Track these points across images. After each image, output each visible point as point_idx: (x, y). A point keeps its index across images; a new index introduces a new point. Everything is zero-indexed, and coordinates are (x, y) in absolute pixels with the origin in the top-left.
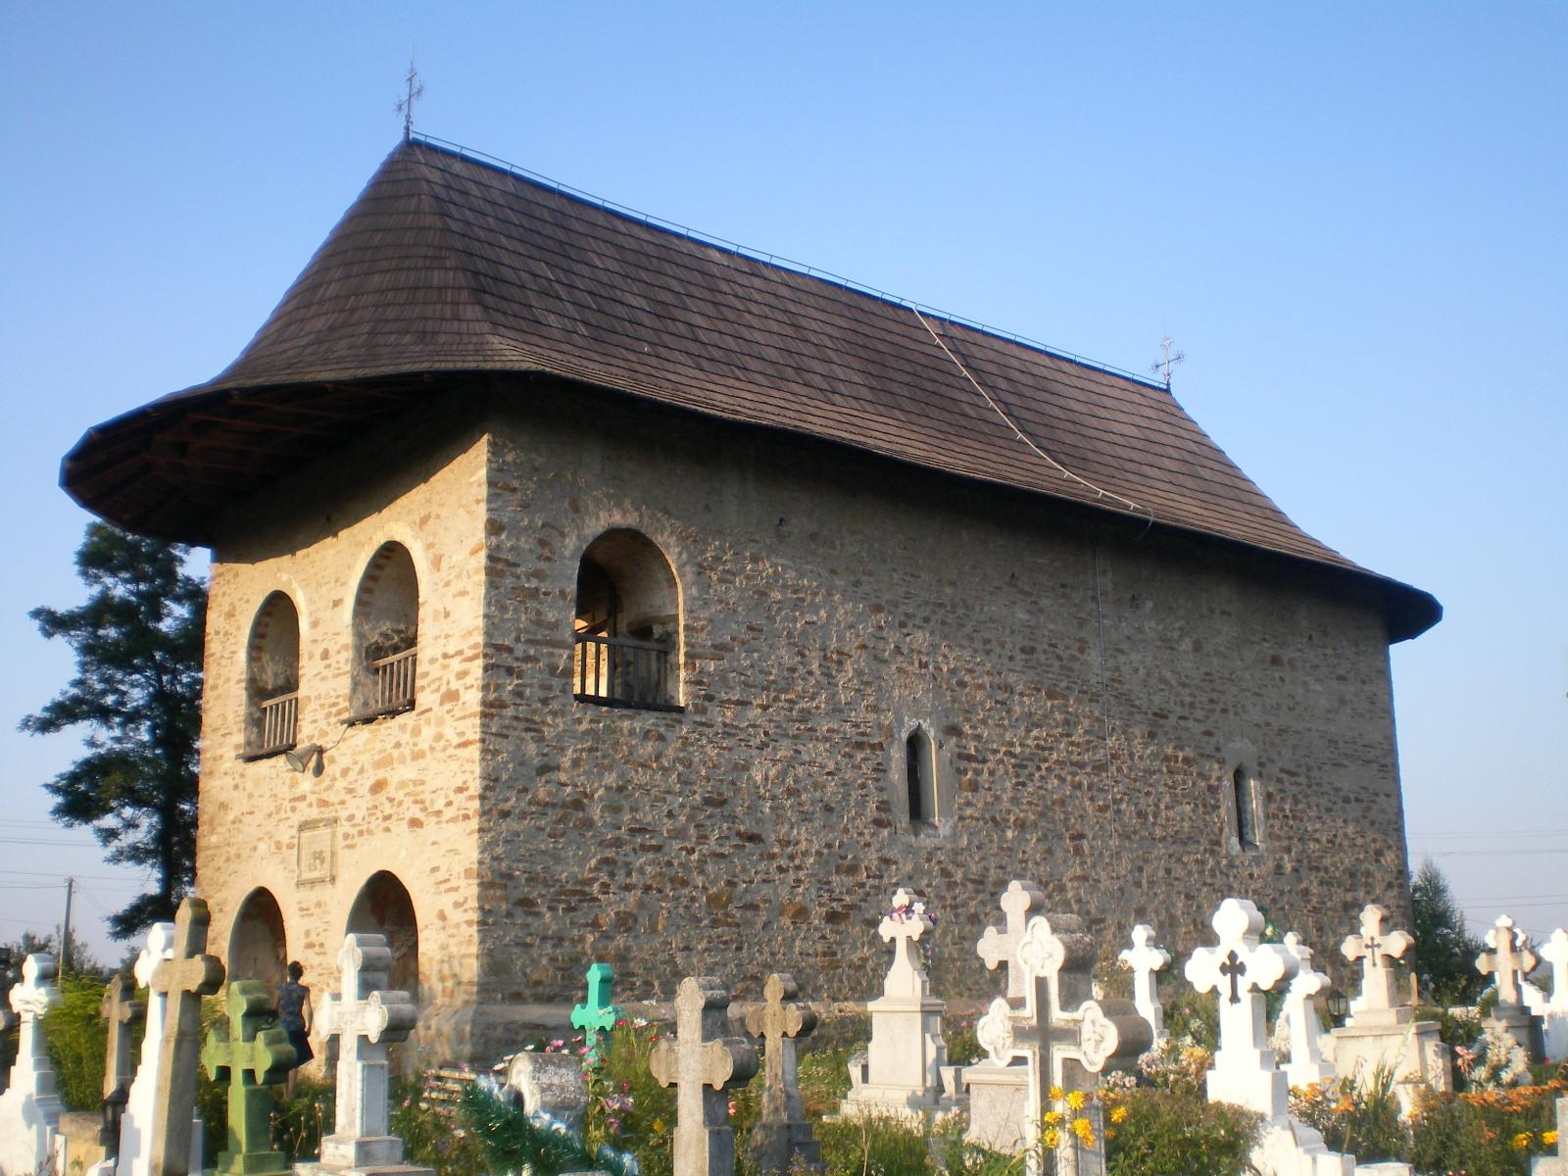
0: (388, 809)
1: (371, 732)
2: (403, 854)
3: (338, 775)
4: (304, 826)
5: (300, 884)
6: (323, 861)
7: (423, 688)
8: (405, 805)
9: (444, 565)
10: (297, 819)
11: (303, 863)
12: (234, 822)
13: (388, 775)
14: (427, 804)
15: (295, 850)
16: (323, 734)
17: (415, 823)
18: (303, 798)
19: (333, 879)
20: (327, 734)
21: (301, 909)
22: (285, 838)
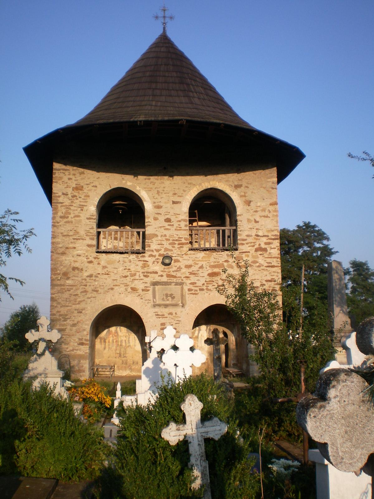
1: (205, 254)
3: (183, 267)
4: (155, 284)
5: (154, 306)
7: (243, 244)
9: (252, 204)
12: (87, 277)
15: (150, 292)
16: (166, 249)
18: (156, 273)
20: (172, 250)
21: (157, 315)
22: (140, 286)
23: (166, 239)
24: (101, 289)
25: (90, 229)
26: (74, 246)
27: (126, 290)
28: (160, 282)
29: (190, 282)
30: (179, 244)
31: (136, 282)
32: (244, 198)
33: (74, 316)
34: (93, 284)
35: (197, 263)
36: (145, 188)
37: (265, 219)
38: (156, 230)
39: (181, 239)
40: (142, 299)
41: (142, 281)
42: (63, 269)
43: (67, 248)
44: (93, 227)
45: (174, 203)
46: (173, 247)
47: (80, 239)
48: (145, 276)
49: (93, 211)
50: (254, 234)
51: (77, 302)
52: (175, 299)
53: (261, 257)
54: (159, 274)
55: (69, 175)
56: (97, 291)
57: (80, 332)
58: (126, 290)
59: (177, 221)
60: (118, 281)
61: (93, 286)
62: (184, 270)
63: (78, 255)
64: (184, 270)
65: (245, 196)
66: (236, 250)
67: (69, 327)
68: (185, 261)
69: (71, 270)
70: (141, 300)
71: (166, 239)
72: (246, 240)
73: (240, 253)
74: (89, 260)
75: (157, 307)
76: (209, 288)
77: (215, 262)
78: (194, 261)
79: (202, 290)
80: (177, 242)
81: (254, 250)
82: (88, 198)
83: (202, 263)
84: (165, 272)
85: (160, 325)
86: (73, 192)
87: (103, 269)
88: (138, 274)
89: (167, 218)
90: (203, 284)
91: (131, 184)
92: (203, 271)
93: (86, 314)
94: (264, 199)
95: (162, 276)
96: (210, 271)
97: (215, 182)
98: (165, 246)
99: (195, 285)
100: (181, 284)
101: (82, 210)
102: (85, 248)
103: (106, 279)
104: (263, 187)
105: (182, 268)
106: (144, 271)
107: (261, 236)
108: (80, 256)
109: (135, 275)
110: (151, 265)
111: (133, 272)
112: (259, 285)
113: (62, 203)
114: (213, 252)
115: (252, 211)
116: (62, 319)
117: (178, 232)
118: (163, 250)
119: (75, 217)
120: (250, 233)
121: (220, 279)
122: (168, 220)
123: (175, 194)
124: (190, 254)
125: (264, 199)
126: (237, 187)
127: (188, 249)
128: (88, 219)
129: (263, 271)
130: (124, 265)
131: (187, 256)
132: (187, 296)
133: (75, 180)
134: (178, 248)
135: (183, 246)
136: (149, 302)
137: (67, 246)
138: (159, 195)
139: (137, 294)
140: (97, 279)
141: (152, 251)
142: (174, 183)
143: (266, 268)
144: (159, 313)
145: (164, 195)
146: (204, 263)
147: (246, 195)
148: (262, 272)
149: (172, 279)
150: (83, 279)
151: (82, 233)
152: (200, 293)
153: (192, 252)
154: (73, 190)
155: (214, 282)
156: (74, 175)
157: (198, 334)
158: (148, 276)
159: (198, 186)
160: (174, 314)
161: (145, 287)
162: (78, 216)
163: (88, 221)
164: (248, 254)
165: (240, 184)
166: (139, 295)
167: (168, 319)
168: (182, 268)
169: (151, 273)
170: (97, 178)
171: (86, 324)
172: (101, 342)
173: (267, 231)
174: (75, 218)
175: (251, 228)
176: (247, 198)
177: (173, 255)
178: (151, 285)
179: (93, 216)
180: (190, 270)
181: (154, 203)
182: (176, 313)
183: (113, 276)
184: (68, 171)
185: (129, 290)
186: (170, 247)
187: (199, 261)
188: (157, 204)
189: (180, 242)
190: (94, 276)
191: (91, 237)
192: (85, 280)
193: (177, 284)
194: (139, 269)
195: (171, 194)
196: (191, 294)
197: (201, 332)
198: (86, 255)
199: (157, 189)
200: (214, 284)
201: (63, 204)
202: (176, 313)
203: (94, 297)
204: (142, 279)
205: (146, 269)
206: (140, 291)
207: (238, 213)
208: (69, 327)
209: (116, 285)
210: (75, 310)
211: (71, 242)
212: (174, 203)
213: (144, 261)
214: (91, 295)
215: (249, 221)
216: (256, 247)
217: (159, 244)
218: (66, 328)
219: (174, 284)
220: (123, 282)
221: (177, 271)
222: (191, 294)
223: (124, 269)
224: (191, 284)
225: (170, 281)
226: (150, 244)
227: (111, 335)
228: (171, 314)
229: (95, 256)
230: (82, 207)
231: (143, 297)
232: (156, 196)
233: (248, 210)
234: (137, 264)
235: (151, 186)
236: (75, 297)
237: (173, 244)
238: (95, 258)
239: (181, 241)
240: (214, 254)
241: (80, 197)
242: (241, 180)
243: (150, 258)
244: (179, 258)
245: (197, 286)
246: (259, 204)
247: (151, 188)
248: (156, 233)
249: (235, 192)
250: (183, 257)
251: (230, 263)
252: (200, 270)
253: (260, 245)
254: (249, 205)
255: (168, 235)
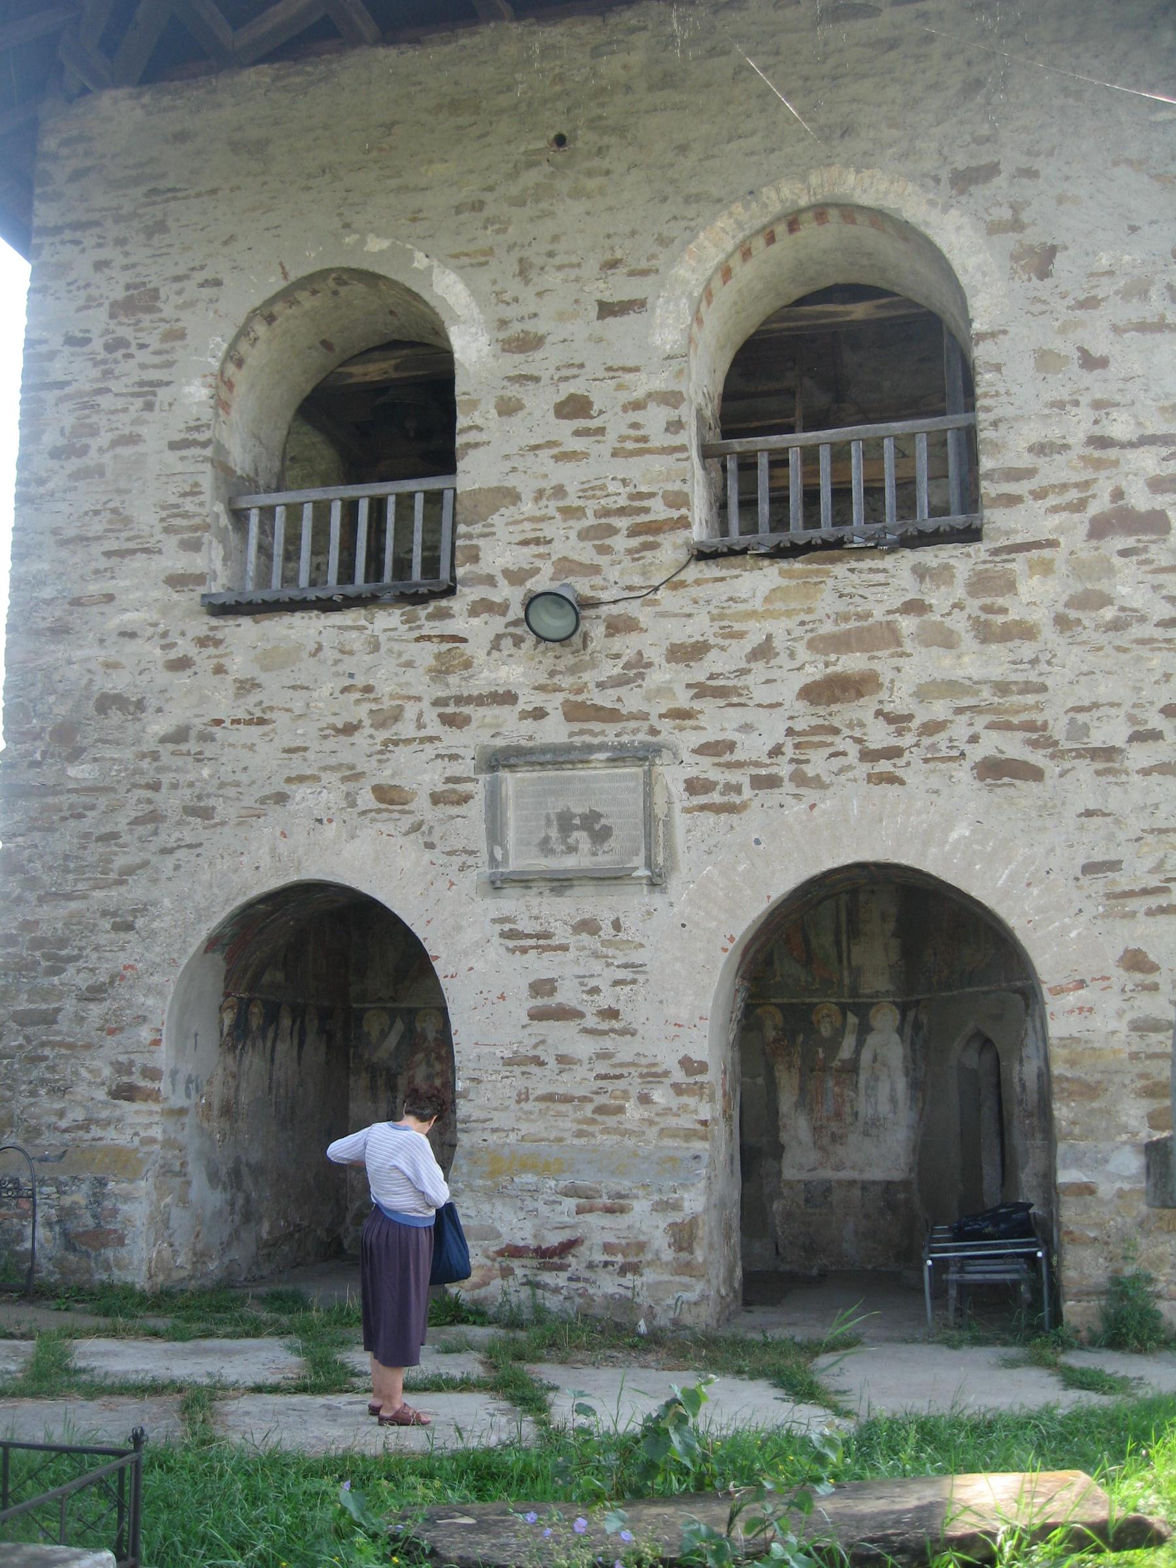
0: (879, 736)
1: (782, 573)
2: (961, 831)
3: (656, 654)
4: (498, 761)
5: (497, 884)
6: (601, 836)
7: (1012, 500)
8: (960, 729)
9: (1060, 262)
10: (469, 742)
11: (511, 836)
12: (164, 740)
13: (876, 666)
14: (1058, 730)
15: (476, 809)
16: (566, 566)
17: (995, 770)
18: (509, 698)
19: (656, 882)
20: (596, 569)
22: (421, 774)
23: (559, 509)
24: (226, 798)
25: (185, 495)
26: (108, 586)
27: (351, 800)
28: (531, 751)
29: (697, 739)
30: (633, 532)
31: (401, 754)
32: (1010, 241)
33: (97, 948)
34: (190, 777)
35: (737, 627)
36: (456, 256)
37: (1149, 339)
38: (509, 465)
39: (645, 503)
40: (430, 846)
41: (430, 750)
42: (56, 710)
43: (77, 602)
44: (196, 484)
45: (607, 310)
46: (604, 550)
47: (133, 552)
48: (449, 721)
49: (199, 404)
50: (1077, 438)
51: (113, 876)
52: (612, 843)
53: (1127, 568)
54: (521, 705)
55: (99, 245)
56: (205, 814)
57: (120, 1029)
58: (351, 800)
59: (625, 409)
60: (310, 755)
61: (191, 785)
62: (661, 675)
63: (123, 634)
64: (661, 675)
65: (1017, 225)
66: (972, 534)
67: (70, 1005)
68: (670, 625)
69: (90, 708)
70: (428, 855)
71: (559, 509)
72: (1030, 473)
73: (996, 552)
74: (173, 655)
75: (509, 891)
76: (810, 771)
77: (846, 618)
78: (721, 617)
79: (772, 782)
80: (622, 523)
81: (1084, 529)
82: (178, 344)
83: (769, 626)
84: (558, 689)
85: (525, 991)
86: (112, 325)
87: (238, 696)
88: (411, 710)
89: (572, 398)
90: (776, 751)
91: (385, 244)
92: (775, 674)
93: (153, 934)
94: (1133, 229)
95: (539, 714)
96: (814, 672)
97: (835, 170)
98: (559, 549)
99: (727, 758)
100: (646, 755)
101: (149, 406)
102: (156, 594)
103: (251, 748)
104: (1129, 162)
105: (649, 665)
106: (441, 693)
107: (1123, 446)
108: (133, 635)
109: (397, 716)
110: (480, 657)
111: (387, 704)
112: (1120, 742)
113: (62, 385)
114: (833, 561)
115: (1060, 306)
116: (45, 964)
117: (633, 469)
118: (547, 569)
119: (115, 443)
120: (1054, 433)
121: (879, 713)
122: (575, 407)
123: (613, 264)
124: (698, 582)
125: (1133, 229)
126: (965, 180)
127: (683, 556)
128: (173, 446)
129: (1144, 652)
130: (340, 668)
131: (681, 592)
132: (680, 821)
133: (126, 268)
134: (629, 551)
135: (660, 538)
136: (470, 860)
137: (76, 594)
138: (527, 283)
139: (407, 822)
140: (209, 750)
141: (490, 581)
142: (610, 209)
143: (1159, 633)
144: (519, 927)
145: (553, 279)
146: (778, 628)
147: (1025, 217)
148: (1139, 659)
149: (596, 726)
150: (143, 756)
151: (146, 518)
152: (756, 804)
153: (710, 570)
154: (112, 316)
155: (836, 731)
156: (121, 242)
157: (858, 1051)
158: (467, 720)
159: (738, 208)
160: (607, 931)
161: (449, 780)
162: (133, 439)
163: (171, 457)
164: (1047, 553)
165: (984, 160)
166: (416, 828)
167: (572, 954)
168: (649, 665)
169: (480, 701)
170: (225, 243)
171: (150, 990)
172: (373, 1087)
173: (1163, 409)
174: (119, 450)
175: (1060, 405)
176: (1032, 237)
177: (604, 596)
178: (478, 769)
179: (197, 428)
180: (699, 673)
181: (503, 323)
182: (617, 925)
183: (285, 732)
184: (97, 230)
185: (367, 799)
186: (585, 553)
187: (752, 614)
188: (515, 329)
189: (643, 518)
190: (193, 733)
191: (186, 536)
192: (155, 756)
193: (621, 756)
194: (420, 682)
195: (592, 266)
196: (702, 808)
197: (872, 1040)
198: (162, 628)
199: (516, 254)
200: (841, 744)
201: (67, 390)
202: (617, 925)
203: (190, 846)
204: (431, 739)
205: (455, 684)
206: (421, 805)
207: (977, 326)
208: (70, 1005)
209: (301, 779)
210: (104, 914)
211: (97, 572)
212: (607, 310)
213: (443, 638)
214: (176, 835)
215: (1046, 361)
216: (1094, 509)
217: (525, 543)
218: (58, 1010)
219: (603, 756)
220: (333, 761)
221: (620, 682)
222: (702, 808)
223: (345, 690)
224: (704, 750)
225: (587, 739)
226: (481, 542)
227: (420, 1056)
228: (588, 926)
229: (203, 631)
230: (147, 391)
231: (435, 838)
232: (514, 287)
233: (1036, 300)
234: (405, 658)
235: (488, 237)
236: (101, 848)
237: (599, 534)
238: (202, 642)
239: (646, 510)
240: (840, 569)
241: (142, 346)
242: (988, 140)
243: (475, 621)
244: (632, 609)
245: (739, 765)
246: (1105, 261)
247: (490, 252)
248: (512, 481)
249: (954, 212)
250: (655, 603)
251: (936, 617)
252: (758, 666)
253: (1118, 494)
254: (1044, 274)
255: (572, 489)
